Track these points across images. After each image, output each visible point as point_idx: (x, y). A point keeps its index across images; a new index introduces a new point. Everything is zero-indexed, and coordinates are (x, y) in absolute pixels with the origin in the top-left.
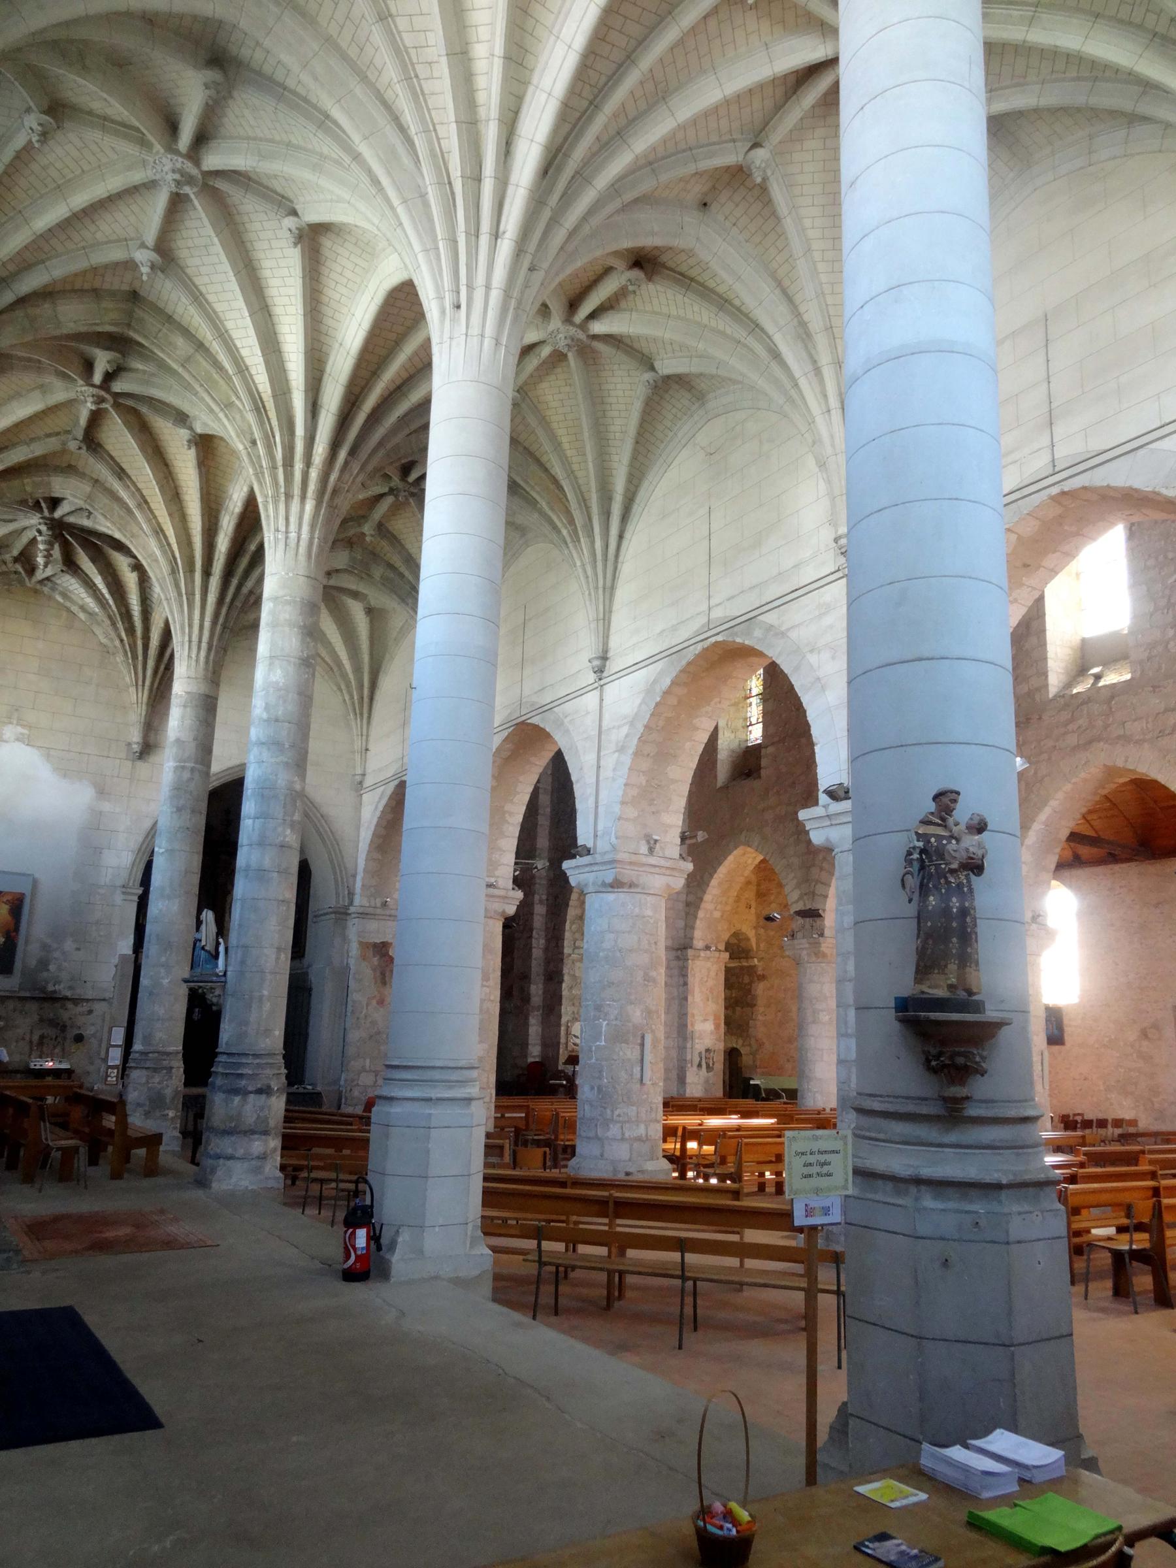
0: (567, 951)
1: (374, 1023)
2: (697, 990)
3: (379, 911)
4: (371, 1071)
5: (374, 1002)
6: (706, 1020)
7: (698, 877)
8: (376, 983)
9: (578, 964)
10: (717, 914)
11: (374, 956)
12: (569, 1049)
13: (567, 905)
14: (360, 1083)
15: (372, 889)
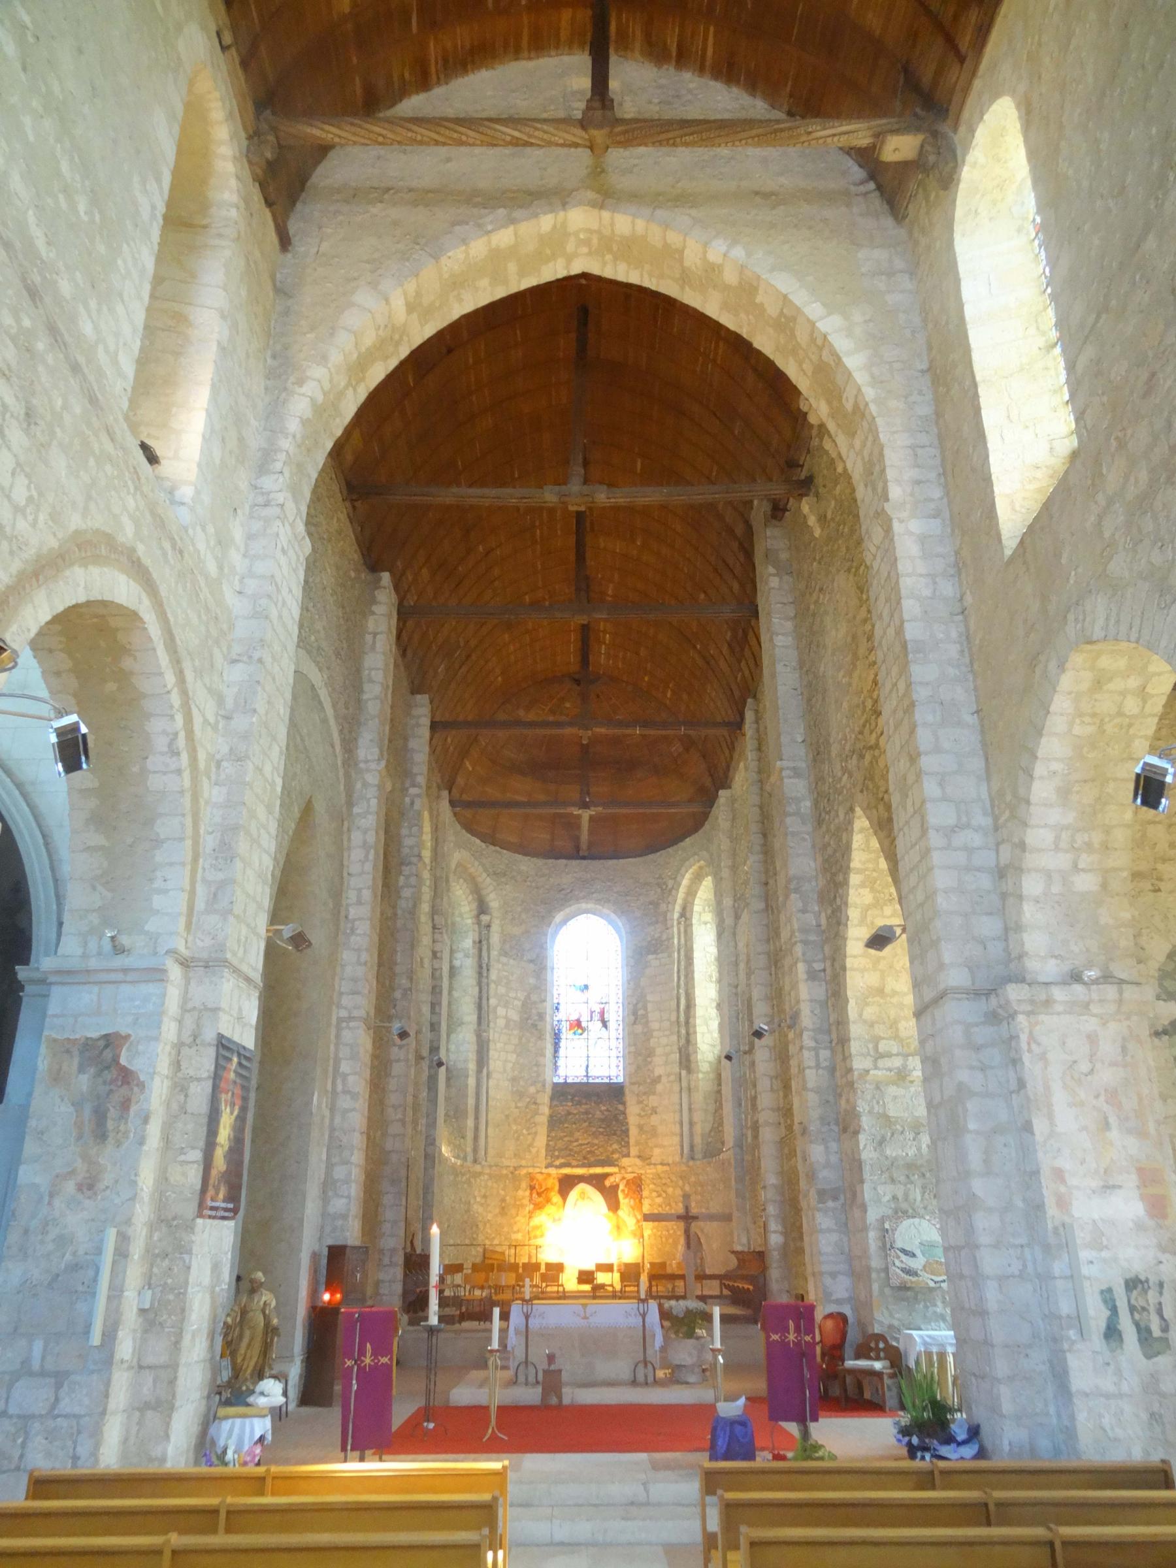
0: (858, 1064)
1: (63, 1241)
2: (1059, 1098)
3: (93, 963)
4: (43, 1374)
5: (70, 1187)
6: (1109, 1188)
7: (1009, 798)
8: (80, 1137)
9: (892, 1090)
10: (1086, 883)
11: (81, 1069)
12: (895, 1282)
13: (844, 968)
14: (12, 1410)
15: (95, 919)
